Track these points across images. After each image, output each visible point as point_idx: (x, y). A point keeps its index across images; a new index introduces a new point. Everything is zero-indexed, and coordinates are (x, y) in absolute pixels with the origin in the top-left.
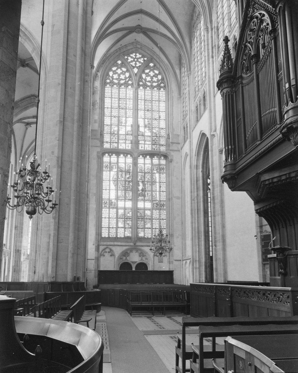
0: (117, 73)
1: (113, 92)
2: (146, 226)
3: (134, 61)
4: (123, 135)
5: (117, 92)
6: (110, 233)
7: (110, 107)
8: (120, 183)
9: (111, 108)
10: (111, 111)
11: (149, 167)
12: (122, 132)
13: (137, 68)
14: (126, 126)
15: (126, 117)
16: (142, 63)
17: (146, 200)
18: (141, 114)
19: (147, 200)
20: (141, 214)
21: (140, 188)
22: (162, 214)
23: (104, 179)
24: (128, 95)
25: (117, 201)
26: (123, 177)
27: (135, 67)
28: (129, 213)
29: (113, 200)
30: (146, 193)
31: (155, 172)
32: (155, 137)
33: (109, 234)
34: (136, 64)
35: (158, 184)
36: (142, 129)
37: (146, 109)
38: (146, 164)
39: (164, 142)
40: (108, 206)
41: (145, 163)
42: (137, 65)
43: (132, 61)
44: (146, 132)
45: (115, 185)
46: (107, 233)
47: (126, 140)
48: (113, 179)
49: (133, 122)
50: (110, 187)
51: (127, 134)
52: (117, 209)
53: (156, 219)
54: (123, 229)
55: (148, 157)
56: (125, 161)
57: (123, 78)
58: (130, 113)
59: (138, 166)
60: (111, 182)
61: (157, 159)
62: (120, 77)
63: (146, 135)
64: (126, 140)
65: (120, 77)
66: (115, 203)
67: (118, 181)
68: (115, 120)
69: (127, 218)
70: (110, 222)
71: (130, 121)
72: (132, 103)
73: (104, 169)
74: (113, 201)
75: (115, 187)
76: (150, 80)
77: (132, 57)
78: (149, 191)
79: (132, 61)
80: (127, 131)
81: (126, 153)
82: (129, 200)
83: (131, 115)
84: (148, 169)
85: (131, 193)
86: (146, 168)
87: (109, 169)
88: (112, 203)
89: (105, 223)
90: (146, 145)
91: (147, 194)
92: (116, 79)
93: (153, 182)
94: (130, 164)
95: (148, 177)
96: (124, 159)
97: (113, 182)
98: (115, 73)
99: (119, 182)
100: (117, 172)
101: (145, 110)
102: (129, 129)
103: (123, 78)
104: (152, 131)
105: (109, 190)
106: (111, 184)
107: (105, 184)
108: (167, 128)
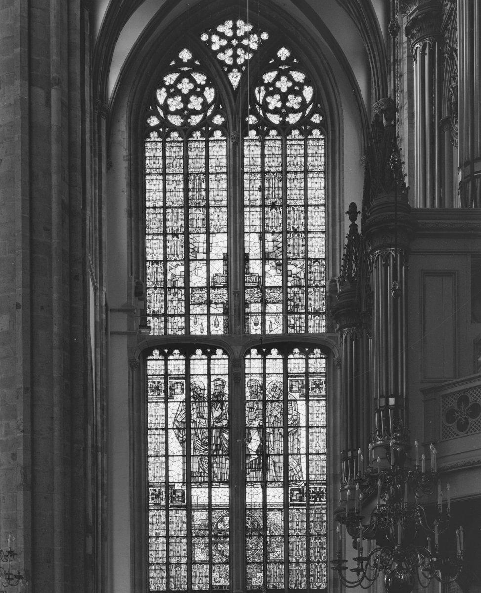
0: (179, 92)
1: (168, 154)
2: (271, 557)
3: (229, 46)
4: (202, 288)
5: (181, 153)
6: (171, 580)
7: (161, 204)
8: (196, 434)
9: (165, 207)
10: (165, 214)
11: (277, 382)
12: (198, 279)
13: (239, 68)
14: (208, 260)
15: (208, 233)
16: (252, 51)
17: (271, 482)
18: (252, 218)
19: (274, 481)
20: (255, 521)
21: (254, 444)
22: (315, 519)
23: (150, 426)
24: (212, 162)
25: (189, 489)
26: (202, 417)
27: (235, 65)
28: (222, 521)
29: (176, 484)
30: (270, 462)
31: (297, 396)
32: (296, 289)
33: (168, 584)
34: (235, 56)
35: (303, 432)
36: (255, 267)
37: (268, 202)
38: (268, 374)
39: (321, 303)
40: (163, 503)
41: (267, 371)
42: (240, 61)
43: (223, 49)
44: (267, 275)
45: (182, 443)
46: (165, 579)
47: (209, 303)
48: (176, 423)
49: (228, 247)
50: (167, 449)
51: (211, 284)
52: (189, 509)
53: (298, 536)
54: (207, 567)
55: (274, 352)
56: (209, 368)
57: (199, 108)
58: (219, 218)
59: (247, 379)
60: (172, 434)
61: (301, 356)
62: (190, 106)
63: (267, 284)
64: (209, 303)
65: (190, 106)
66: (183, 494)
67: (188, 428)
68: (176, 245)
69: (216, 536)
70: (171, 547)
71: (220, 244)
72: (225, 186)
73: (150, 395)
74: (178, 487)
75: (183, 447)
76: (279, 105)
77: (222, 36)
78: (279, 455)
79: (223, 49)
80: (211, 275)
81: (209, 345)
82: (221, 482)
83: (224, 223)
84: (273, 389)
85: (227, 461)
86: (268, 386)
87: (163, 395)
88: (175, 494)
89: (156, 550)
90: (267, 317)
91: (271, 463)
92: (176, 113)
93: (288, 429)
94: (223, 377)
95: (274, 413)
96: (206, 361)
97: (176, 431)
98: (173, 92)
99: (192, 432)
100: (187, 401)
101: (263, 206)
102: (218, 268)
103: (199, 108)
104: (287, 271)
105: (167, 456)
106: (170, 441)
107: (154, 441)
108: (331, 258)
